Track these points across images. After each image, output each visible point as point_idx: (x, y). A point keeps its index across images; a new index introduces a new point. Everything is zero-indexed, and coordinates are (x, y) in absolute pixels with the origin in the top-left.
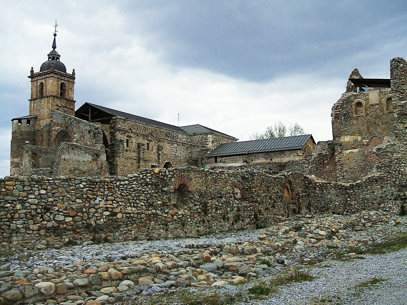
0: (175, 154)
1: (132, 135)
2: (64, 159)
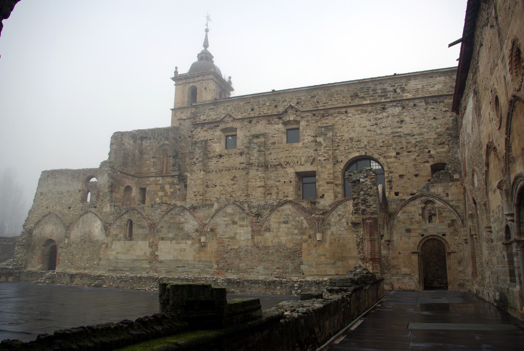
0: (393, 133)
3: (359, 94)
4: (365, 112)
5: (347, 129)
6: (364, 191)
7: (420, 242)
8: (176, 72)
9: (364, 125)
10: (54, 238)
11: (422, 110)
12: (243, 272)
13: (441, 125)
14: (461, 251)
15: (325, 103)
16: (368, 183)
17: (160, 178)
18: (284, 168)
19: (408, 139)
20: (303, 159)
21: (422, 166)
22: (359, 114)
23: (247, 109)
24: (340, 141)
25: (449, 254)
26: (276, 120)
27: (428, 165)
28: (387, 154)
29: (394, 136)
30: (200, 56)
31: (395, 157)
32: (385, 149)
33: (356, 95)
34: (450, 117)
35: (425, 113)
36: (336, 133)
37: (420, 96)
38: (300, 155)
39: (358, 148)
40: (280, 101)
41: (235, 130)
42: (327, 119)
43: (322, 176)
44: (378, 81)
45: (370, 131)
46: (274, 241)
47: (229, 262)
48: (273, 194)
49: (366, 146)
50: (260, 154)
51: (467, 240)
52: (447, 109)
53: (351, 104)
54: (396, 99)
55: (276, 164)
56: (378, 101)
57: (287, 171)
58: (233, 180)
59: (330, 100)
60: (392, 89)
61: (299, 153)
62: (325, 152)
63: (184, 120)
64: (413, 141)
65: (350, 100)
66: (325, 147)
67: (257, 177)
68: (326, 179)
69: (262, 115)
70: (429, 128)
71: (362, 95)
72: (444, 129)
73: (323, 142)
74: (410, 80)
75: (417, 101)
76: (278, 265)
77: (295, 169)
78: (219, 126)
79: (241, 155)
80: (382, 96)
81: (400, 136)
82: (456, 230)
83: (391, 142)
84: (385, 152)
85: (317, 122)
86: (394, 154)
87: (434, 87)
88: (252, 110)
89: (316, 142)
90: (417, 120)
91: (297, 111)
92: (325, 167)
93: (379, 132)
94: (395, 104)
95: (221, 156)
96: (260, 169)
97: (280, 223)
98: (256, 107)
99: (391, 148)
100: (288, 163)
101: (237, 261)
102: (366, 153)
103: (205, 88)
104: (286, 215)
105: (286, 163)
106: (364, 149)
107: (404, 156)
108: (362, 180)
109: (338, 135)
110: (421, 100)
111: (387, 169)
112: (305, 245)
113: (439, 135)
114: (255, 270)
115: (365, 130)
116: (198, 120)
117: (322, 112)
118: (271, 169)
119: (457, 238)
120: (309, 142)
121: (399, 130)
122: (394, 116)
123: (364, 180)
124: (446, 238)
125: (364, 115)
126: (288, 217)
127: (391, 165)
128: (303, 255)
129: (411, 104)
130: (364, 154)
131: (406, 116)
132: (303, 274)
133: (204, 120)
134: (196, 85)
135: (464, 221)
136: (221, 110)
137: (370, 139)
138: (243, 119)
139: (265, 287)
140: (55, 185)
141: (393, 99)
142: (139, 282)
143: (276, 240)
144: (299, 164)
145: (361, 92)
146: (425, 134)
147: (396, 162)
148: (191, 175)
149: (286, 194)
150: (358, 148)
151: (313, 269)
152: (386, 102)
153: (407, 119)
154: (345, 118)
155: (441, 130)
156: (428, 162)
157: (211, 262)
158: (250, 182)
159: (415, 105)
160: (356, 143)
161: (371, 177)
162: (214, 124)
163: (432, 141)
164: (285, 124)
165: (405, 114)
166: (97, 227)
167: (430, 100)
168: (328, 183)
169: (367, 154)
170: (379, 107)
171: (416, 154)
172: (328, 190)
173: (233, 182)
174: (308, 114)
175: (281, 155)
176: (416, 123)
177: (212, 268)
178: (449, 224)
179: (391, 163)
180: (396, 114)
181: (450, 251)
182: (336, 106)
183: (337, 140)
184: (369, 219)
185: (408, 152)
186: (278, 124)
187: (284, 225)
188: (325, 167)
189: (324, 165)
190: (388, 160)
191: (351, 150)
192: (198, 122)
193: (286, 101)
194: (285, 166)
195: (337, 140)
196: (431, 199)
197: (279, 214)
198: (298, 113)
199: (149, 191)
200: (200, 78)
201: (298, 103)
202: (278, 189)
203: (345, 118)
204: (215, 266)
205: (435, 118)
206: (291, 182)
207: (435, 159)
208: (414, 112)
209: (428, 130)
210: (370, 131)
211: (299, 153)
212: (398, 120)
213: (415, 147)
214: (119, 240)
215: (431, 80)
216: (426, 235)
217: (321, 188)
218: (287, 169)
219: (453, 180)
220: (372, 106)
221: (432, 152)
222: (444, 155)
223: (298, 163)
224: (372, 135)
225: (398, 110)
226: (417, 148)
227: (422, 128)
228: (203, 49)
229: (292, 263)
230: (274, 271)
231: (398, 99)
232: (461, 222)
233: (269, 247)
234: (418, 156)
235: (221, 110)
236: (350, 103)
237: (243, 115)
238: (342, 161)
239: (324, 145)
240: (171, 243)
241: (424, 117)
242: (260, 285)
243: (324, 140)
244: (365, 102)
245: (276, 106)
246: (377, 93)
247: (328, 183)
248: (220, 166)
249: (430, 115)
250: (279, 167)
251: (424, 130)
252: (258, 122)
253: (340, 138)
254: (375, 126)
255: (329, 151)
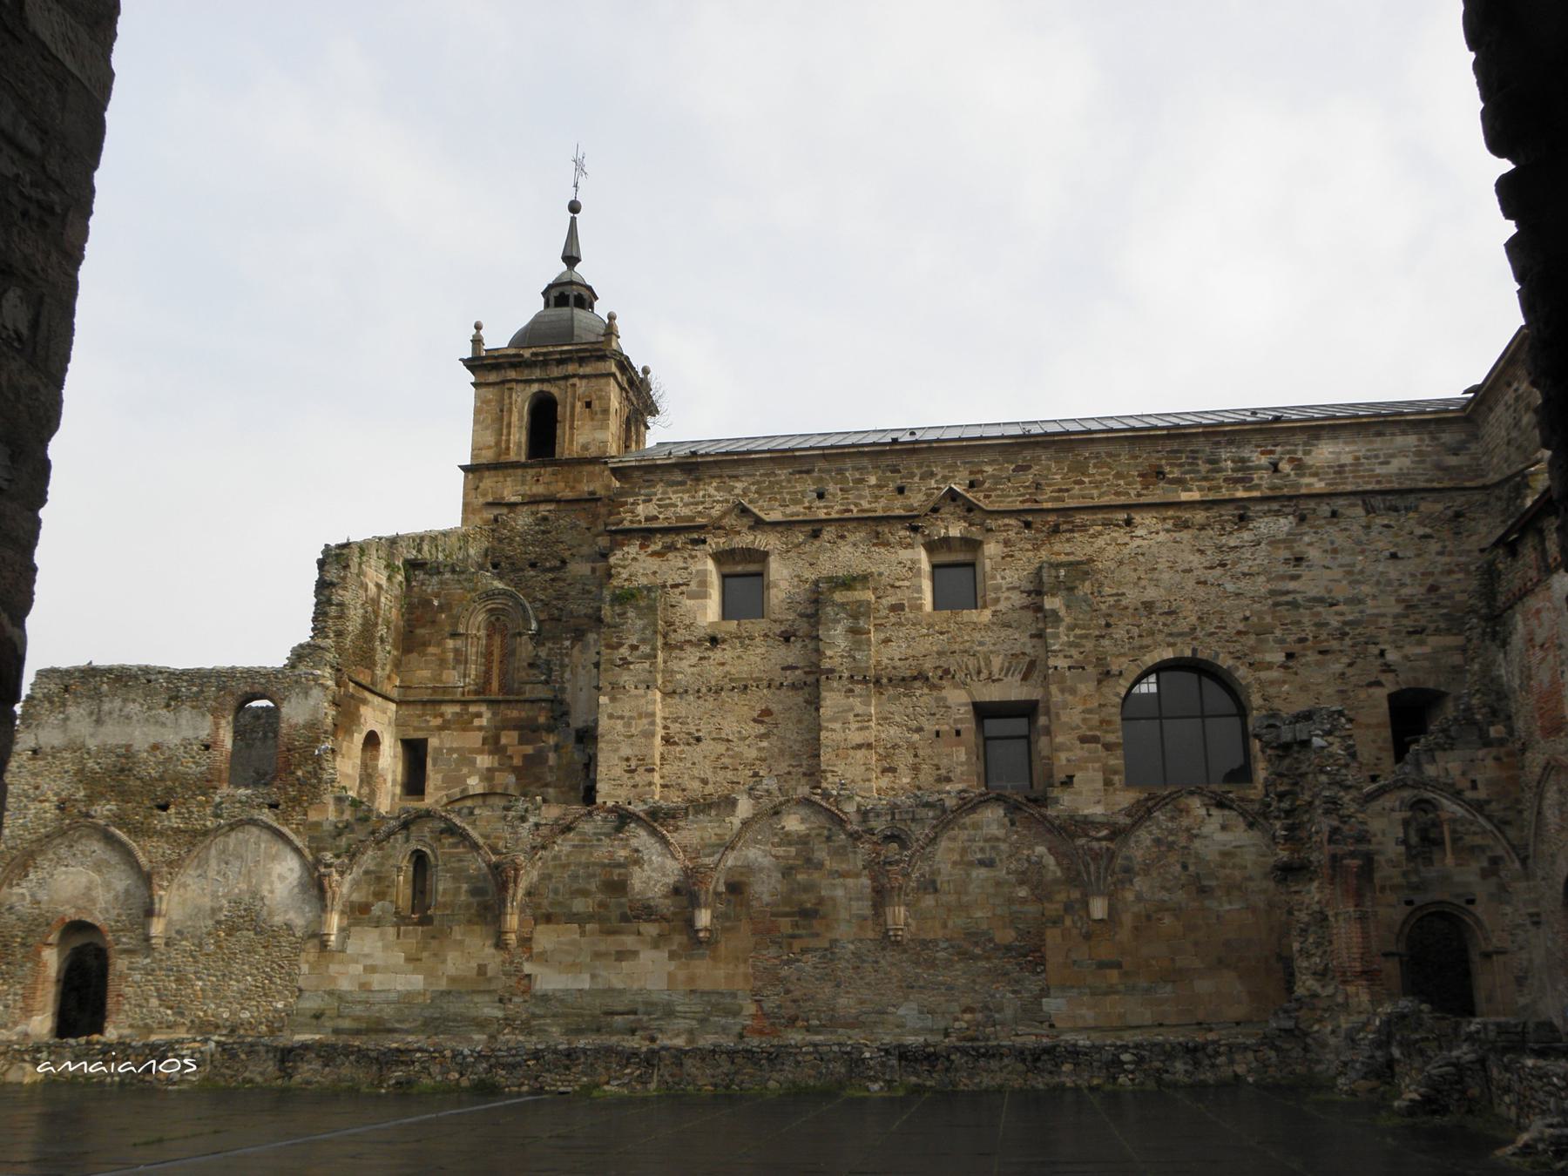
0: (1273, 593)
1: (762, 541)
2: (35, 752)
3: (1167, 469)
4: (1184, 525)
5: (1134, 576)
6: (1327, 773)
7: (1404, 923)
8: (477, 341)
9: (1187, 566)
10: (97, 918)
11: (1356, 530)
12: (852, 1026)
13: (1413, 575)
14: (1521, 948)
15: (1060, 490)
16: (1337, 749)
17: (483, 708)
18: (933, 687)
19: (1319, 614)
20: (997, 662)
21: (1362, 695)
22: (1168, 531)
23: (803, 493)
24: (1115, 612)
25: (1487, 956)
26: (902, 533)
27: (1381, 694)
28: (1258, 657)
29: (1276, 604)
30: (555, 293)
31: (1284, 666)
32: (1251, 640)
33: (1160, 474)
34: (1440, 553)
35: (1364, 538)
36: (1101, 585)
37: (1349, 488)
38: (984, 649)
39: (1171, 635)
40: (912, 475)
41: (763, 556)
42: (1068, 540)
43: (1064, 718)
44: (1225, 433)
45: (1205, 583)
46: (950, 924)
47: (797, 994)
48: (902, 768)
49: (1194, 629)
50: (854, 642)
51: (1538, 915)
52: (1428, 531)
53: (1142, 500)
54: (1277, 493)
55: (908, 674)
56: (1225, 494)
57: (944, 699)
58: (762, 722)
59: (1076, 483)
60: (1264, 460)
61: (981, 644)
62: (1071, 645)
63: (512, 506)
64: (1335, 622)
65: (1139, 486)
66: (1071, 628)
67: (851, 717)
68: (1078, 727)
69: (855, 514)
70: (1378, 583)
71: (1176, 473)
72: (1423, 590)
73: (1062, 613)
74: (1318, 438)
75: (1341, 502)
76: (967, 1001)
77: (970, 694)
78: (704, 542)
79: (787, 640)
80: (1237, 481)
81: (1294, 605)
82: (1503, 888)
83: (1268, 619)
84: (1253, 649)
85: (1036, 548)
86: (1279, 657)
87: (1387, 463)
88: (821, 496)
89: (1039, 608)
90: (1344, 559)
91: (970, 510)
92: (1073, 691)
93: (1230, 587)
94: (1275, 506)
95: (714, 641)
96: (858, 688)
97: (971, 864)
98: (831, 488)
99: (1270, 637)
100: (947, 671)
101: (828, 989)
102: (1194, 650)
103: (588, 405)
104: (986, 841)
105: (940, 673)
106: (1188, 639)
107: (1307, 664)
108: (1317, 742)
109: (1107, 590)
110: (1353, 500)
111: (1261, 702)
112: (1053, 936)
113: (1410, 606)
114: (891, 1018)
115: (1190, 584)
116: (629, 516)
117: (1052, 518)
118: (891, 691)
119: (1509, 909)
120: (1013, 609)
121: (1292, 585)
122: (1274, 542)
123: (1323, 743)
124: (1478, 909)
125: (1185, 535)
126: (993, 848)
127: (1272, 691)
128: (1049, 967)
129: (1325, 509)
130: (1188, 653)
131: (1310, 544)
132: (1052, 1026)
133: (647, 519)
134: (555, 391)
135: (1530, 861)
136: (712, 491)
137: (1206, 608)
138: (787, 525)
139: (1021, 1067)
140: (99, 722)
141: (1269, 493)
142: (567, 1068)
143: (957, 921)
144: (983, 676)
145: (1171, 465)
146: (1369, 602)
147: (1284, 682)
148: (613, 699)
149: (943, 772)
150: (1171, 635)
151: (1084, 1011)
152: (1249, 499)
153: (1313, 554)
154: (1127, 539)
155: (1412, 590)
156: (1378, 684)
157: (734, 995)
158: (827, 729)
159: (1334, 514)
160: (1162, 619)
161: (1344, 733)
162: (691, 533)
163: (1389, 622)
164: (931, 547)
165: (1306, 539)
166: (281, 877)
167: (1377, 502)
168: (1084, 740)
169: (1199, 656)
170: (1228, 512)
171: (1346, 660)
172: (1087, 760)
173: (762, 729)
174: (1007, 521)
175: (925, 646)
176: (1341, 566)
177: (736, 1014)
178: (1483, 869)
179: (1272, 683)
180: (1281, 536)
181: (1490, 948)
182: (1096, 502)
183: (1103, 607)
184: (1352, 855)
185: (1321, 652)
186: (910, 546)
187: (983, 872)
188: (1073, 691)
189: (1069, 683)
190: (1263, 675)
191: (1147, 641)
192: (626, 524)
193: (932, 474)
194: (936, 681)
195: (1103, 607)
196: (1429, 795)
197: (964, 835)
198: (976, 516)
199: (438, 750)
200: (571, 368)
201: (972, 485)
202: (916, 756)
203: (1127, 539)
204: (751, 1008)
205: (1394, 556)
206: (958, 733)
207: (1402, 677)
208: (1333, 533)
209: (1375, 590)
210: (1205, 583)
211: (981, 644)
212: (1287, 554)
213: (1342, 639)
214: (378, 923)
215: (1378, 443)
216: (1419, 899)
217: (1063, 756)
218: (944, 693)
219: (1487, 743)
220: (1207, 509)
221: (1392, 656)
222: (1426, 664)
223: (979, 672)
224: (1212, 597)
225: (1284, 524)
226: (1348, 641)
227: (1358, 582)
228: (564, 267)
229: (1014, 992)
230: (956, 1019)
231: (1285, 491)
232: (1517, 865)
233: (935, 942)
234: (1350, 665)
235: (712, 491)
236: (1139, 495)
237: (788, 511)
238: (1121, 673)
239: (1068, 620)
240: (583, 934)
241: (1362, 552)
242: (1006, 1061)
243: (1068, 607)
244: (1184, 496)
245: (901, 490)
246: (1220, 470)
247: (1084, 740)
248: (714, 673)
249: (1380, 545)
250: (918, 684)
251: (1365, 589)
252: (843, 537)
253: (1111, 600)
254: (1219, 571)
255: (1084, 641)
